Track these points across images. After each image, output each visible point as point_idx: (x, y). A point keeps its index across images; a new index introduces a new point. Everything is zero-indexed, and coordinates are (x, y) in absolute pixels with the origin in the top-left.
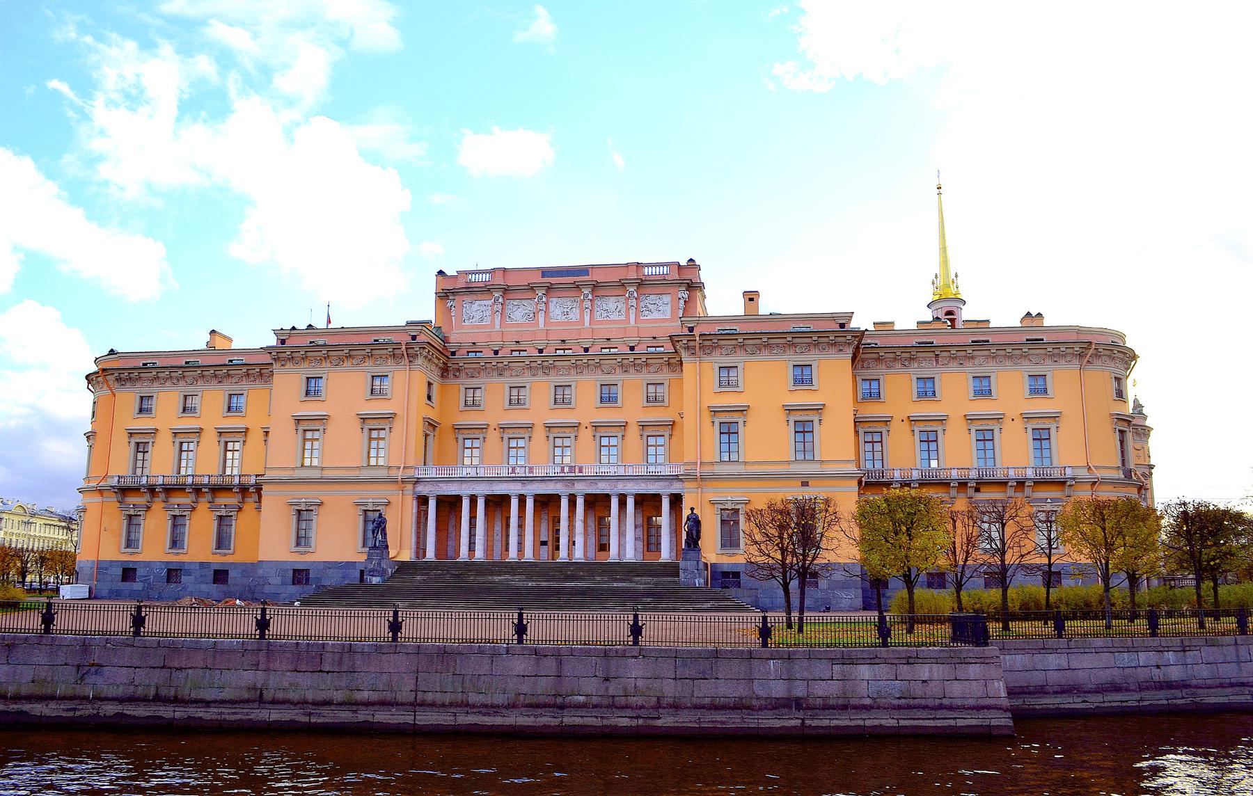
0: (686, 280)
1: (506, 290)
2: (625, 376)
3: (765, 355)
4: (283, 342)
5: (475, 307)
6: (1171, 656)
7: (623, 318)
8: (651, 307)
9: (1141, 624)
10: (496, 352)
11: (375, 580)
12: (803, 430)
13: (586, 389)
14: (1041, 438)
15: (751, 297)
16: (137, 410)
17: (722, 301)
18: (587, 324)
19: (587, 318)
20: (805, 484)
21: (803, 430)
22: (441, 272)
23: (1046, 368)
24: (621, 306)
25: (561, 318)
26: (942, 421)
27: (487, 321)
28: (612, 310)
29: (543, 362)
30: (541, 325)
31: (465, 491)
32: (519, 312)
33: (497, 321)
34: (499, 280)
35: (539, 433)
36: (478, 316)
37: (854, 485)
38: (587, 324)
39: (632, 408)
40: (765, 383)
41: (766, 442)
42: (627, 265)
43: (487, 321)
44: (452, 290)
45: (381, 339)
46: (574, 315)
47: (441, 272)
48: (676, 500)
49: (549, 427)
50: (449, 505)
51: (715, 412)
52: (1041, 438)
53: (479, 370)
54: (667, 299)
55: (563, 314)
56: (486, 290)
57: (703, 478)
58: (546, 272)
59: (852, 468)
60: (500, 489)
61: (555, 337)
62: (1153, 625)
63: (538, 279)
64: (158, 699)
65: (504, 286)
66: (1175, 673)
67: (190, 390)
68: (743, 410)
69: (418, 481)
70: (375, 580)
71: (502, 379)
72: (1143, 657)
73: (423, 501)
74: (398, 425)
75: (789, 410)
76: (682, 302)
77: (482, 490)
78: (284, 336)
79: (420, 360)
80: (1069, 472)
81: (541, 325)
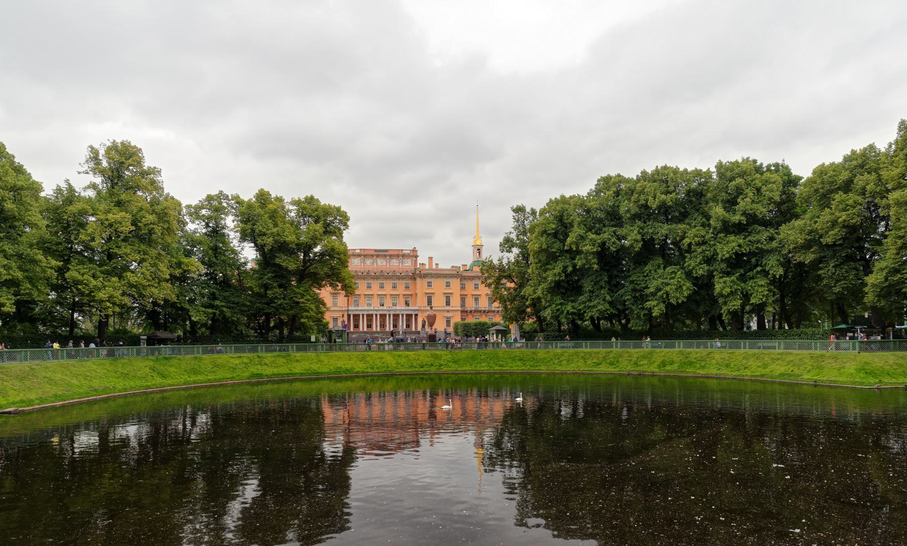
0: (414, 255)
3: (439, 279)
13: (388, 284)
15: (431, 258)
17: (422, 259)
28: (395, 262)
29: (376, 277)
31: (361, 313)
32: (369, 262)
35: (375, 297)
37: (459, 313)
40: (439, 287)
41: (439, 302)
46: (384, 264)
48: (416, 315)
50: (356, 317)
56: (359, 255)
58: (376, 251)
60: (370, 313)
61: (379, 270)
63: (373, 253)
73: (349, 316)
77: (365, 313)
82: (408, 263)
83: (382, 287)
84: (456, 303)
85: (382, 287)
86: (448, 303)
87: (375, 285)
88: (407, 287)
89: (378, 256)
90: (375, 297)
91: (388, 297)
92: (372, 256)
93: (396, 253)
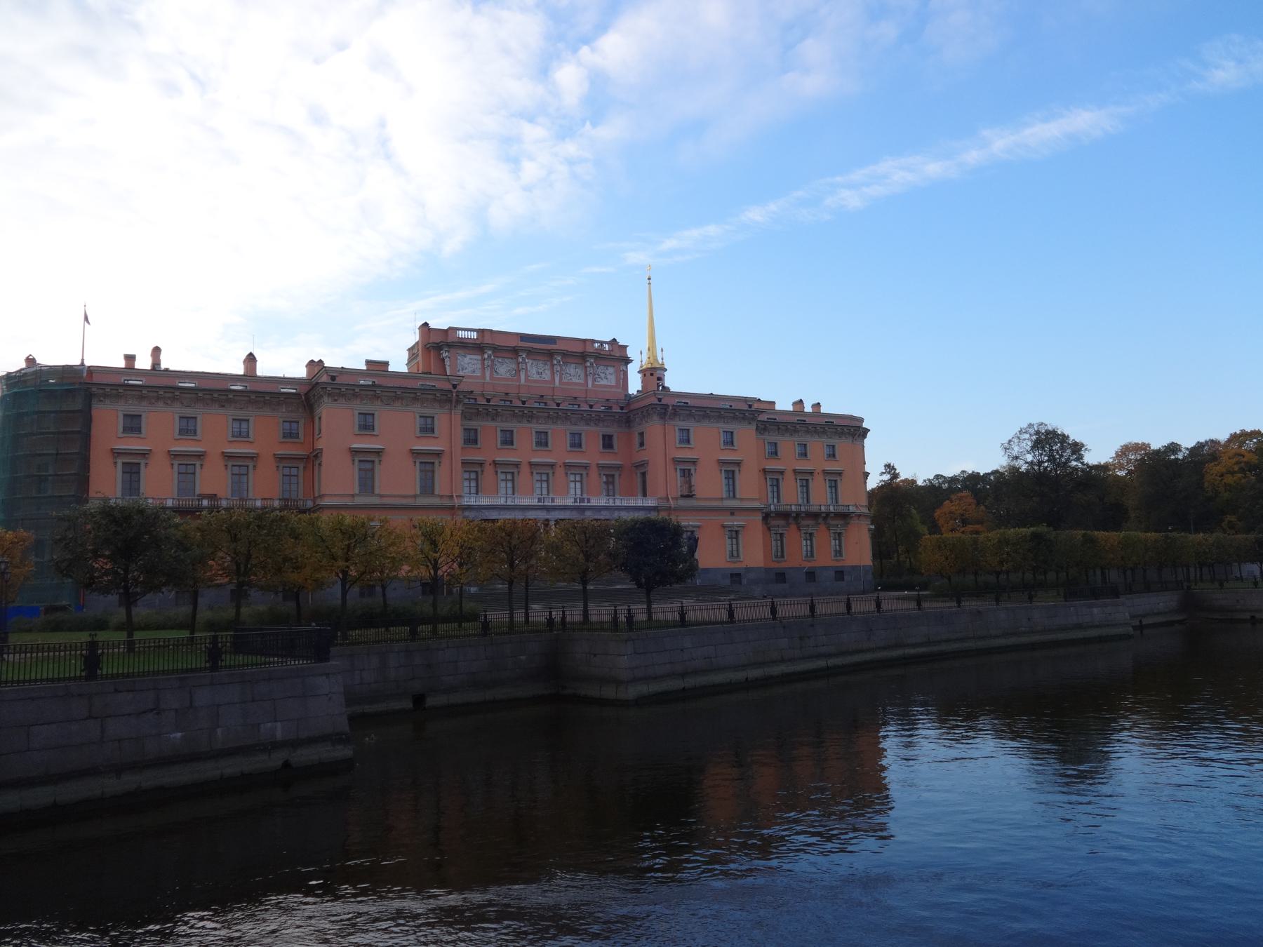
1: (496, 349)
2: (586, 428)
5: (467, 359)
7: (582, 382)
9: (1217, 585)
10: (488, 400)
11: (473, 590)
12: (731, 476)
13: (559, 434)
14: (834, 486)
16: (121, 428)
20: (732, 514)
21: (731, 476)
22: (426, 324)
23: (835, 441)
24: (580, 371)
25: (536, 377)
26: (782, 473)
27: (478, 374)
28: (573, 375)
29: (527, 415)
30: (523, 381)
32: (504, 369)
34: (488, 340)
35: (525, 469)
37: (759, 518)
39: (593, 454)
40: (706, 441)
41: (709, 485)
42: (584, 341)
43: (478, 374)
44: (436, 344)
46: (547, 376)
47: (426, 324)
49: (531, 464)
52: (834, 486)
53: (478, 413)
54: (611, 370)
55: (536, 372)
57: (676, 509)
59: (756, 505)
62: (1221, 585)
64: (948, 641)
65: (489, 344)
68: (694, 462)
69: (469, 508)
70: (473, 590)
71: (493, 424)
75: (722, 463)
80: (852, 509)
81: (523, 381)
82: (607, 378)
83: (542, 441)
84: (750, 490)
85: (542, 441)
86: (733, 494)
87: (525, 433)
88: (608, 442)
89: (531, 353)
90: (525, 469)
91: (560, 471)
92: (515, 351)
93: (579, 349)
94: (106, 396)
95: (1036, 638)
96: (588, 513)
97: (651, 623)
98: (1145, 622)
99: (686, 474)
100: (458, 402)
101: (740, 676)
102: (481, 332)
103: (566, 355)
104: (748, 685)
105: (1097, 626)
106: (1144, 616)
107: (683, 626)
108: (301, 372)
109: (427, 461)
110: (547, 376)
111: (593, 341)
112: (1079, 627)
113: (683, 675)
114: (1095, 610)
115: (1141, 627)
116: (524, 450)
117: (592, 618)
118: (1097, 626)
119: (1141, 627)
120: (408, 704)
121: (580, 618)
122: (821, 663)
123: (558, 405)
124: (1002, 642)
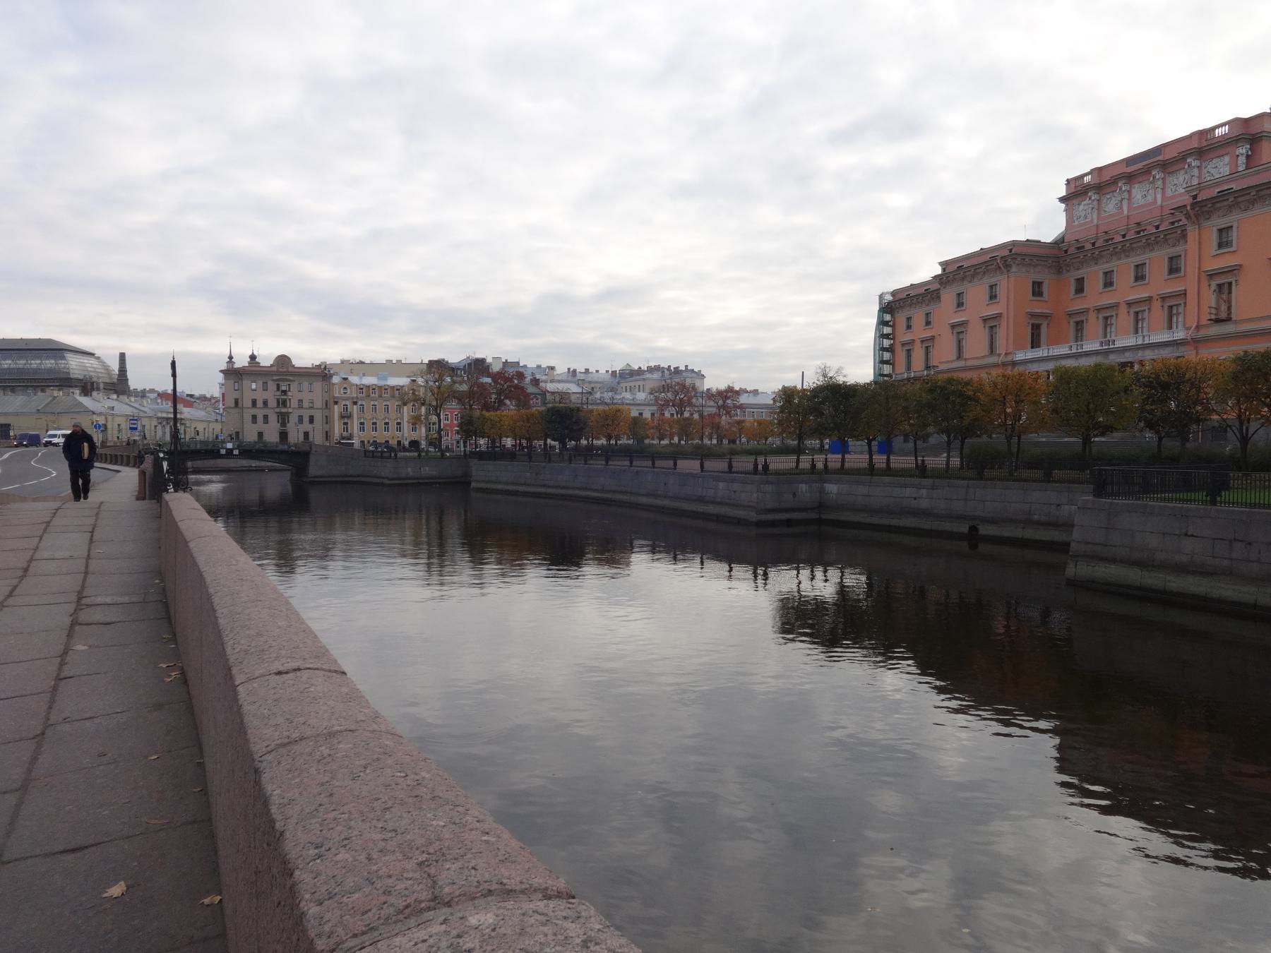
4: (944, 270)
5: (1081, 207)
6: (924, 492)
8: (1213, 171)
10: (1093, 244)
13: (1157, 260)
18: (1159, 202)
19: (1159, 197)
25: (1141, 202)
29: (1124, 249)
32: (1110, 206)
33: (1095, 216)
35: (1123, 309)
36: (1082, 214)
38: (1159, 202)
45: (966, 264)
51: (1211, 276)
54: (1227, 159)
58: (1129, 161)
66: (924, 504)
67: (928, 309)
71: (1096, 268)
72: (908, 492)
74: (1004, 322)
76: (1242, 160)
78: (945, 265)
79: (1014, 269)
87: (1124, 269)
89: (1130, 178)
90: (1123, 309)
94: (902, 307)
95: (667, 503)
96: (1112, 357)
97: (889, 471)
98: (985, 530)
99: (1224, 290)
100: (1010, 266)
101: (507, 487)
102: (1091, 172)
103: (1182, 158)
104: (510, 493)
105: (719, 503)
106: (985, 520)
107: (872, 475)
108: (939, 271)
109: (991, 323)
110: (1150, 198)
111: (1201, 133)
112: (701, 500)
113: (488, 482)
114: (721, 485)
115: (973, 537)
116: (1126, 289)
117: (892, 465)
118: (719, 503)
119: (973, 537)
120: (964, 529)
121: (884, 466)
122: (543, 490)
123: (1157, 227)
124: (644, 500)
